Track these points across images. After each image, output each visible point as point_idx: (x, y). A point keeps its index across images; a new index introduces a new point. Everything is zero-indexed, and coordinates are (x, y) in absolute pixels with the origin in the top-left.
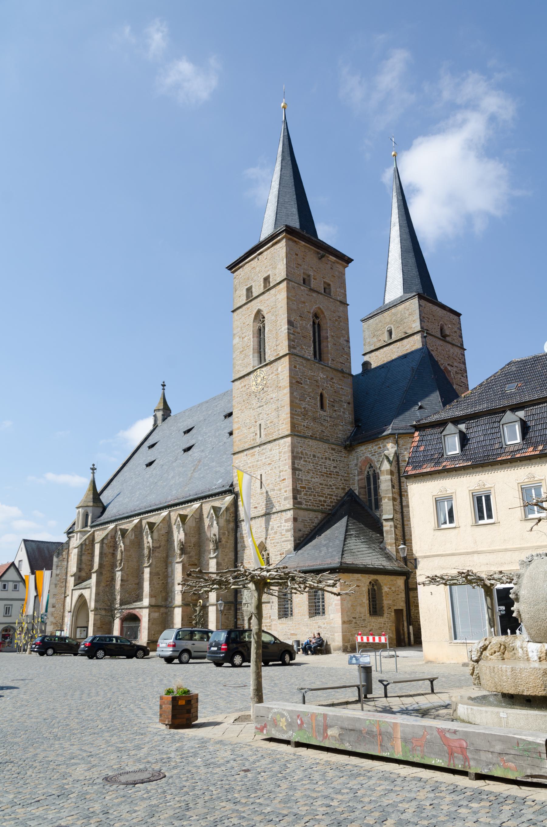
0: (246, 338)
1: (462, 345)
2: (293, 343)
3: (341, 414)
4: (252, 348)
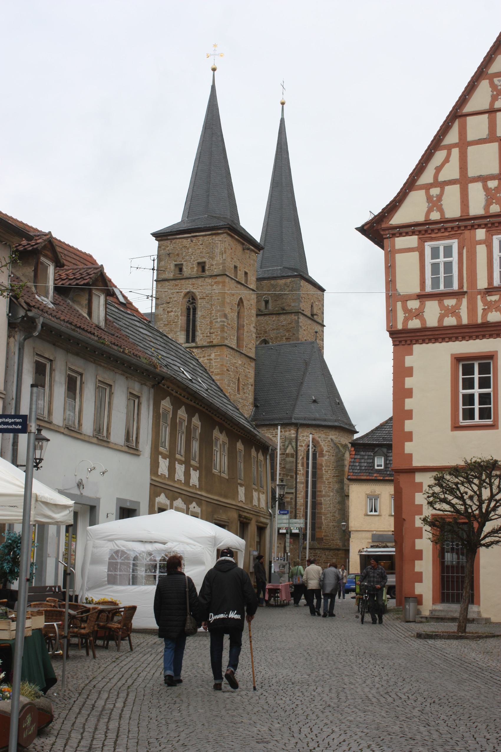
0: (172, 314)
1: (323, 321)
2: (226, 334)
3: (247, 395)
4: (180, 326)
